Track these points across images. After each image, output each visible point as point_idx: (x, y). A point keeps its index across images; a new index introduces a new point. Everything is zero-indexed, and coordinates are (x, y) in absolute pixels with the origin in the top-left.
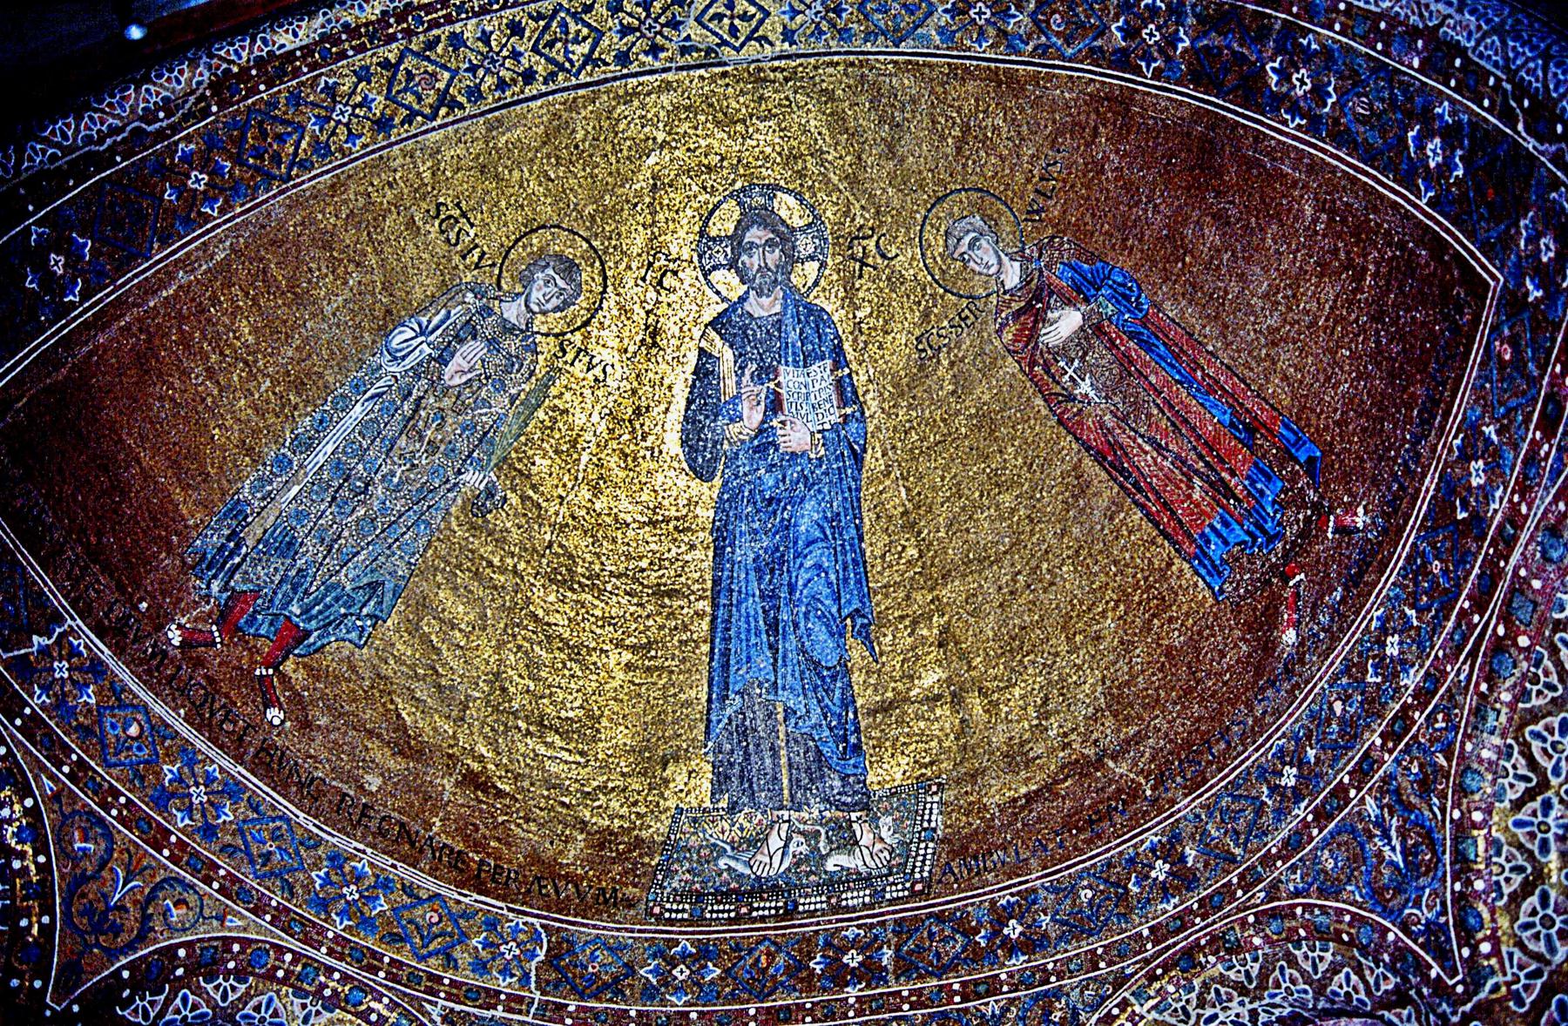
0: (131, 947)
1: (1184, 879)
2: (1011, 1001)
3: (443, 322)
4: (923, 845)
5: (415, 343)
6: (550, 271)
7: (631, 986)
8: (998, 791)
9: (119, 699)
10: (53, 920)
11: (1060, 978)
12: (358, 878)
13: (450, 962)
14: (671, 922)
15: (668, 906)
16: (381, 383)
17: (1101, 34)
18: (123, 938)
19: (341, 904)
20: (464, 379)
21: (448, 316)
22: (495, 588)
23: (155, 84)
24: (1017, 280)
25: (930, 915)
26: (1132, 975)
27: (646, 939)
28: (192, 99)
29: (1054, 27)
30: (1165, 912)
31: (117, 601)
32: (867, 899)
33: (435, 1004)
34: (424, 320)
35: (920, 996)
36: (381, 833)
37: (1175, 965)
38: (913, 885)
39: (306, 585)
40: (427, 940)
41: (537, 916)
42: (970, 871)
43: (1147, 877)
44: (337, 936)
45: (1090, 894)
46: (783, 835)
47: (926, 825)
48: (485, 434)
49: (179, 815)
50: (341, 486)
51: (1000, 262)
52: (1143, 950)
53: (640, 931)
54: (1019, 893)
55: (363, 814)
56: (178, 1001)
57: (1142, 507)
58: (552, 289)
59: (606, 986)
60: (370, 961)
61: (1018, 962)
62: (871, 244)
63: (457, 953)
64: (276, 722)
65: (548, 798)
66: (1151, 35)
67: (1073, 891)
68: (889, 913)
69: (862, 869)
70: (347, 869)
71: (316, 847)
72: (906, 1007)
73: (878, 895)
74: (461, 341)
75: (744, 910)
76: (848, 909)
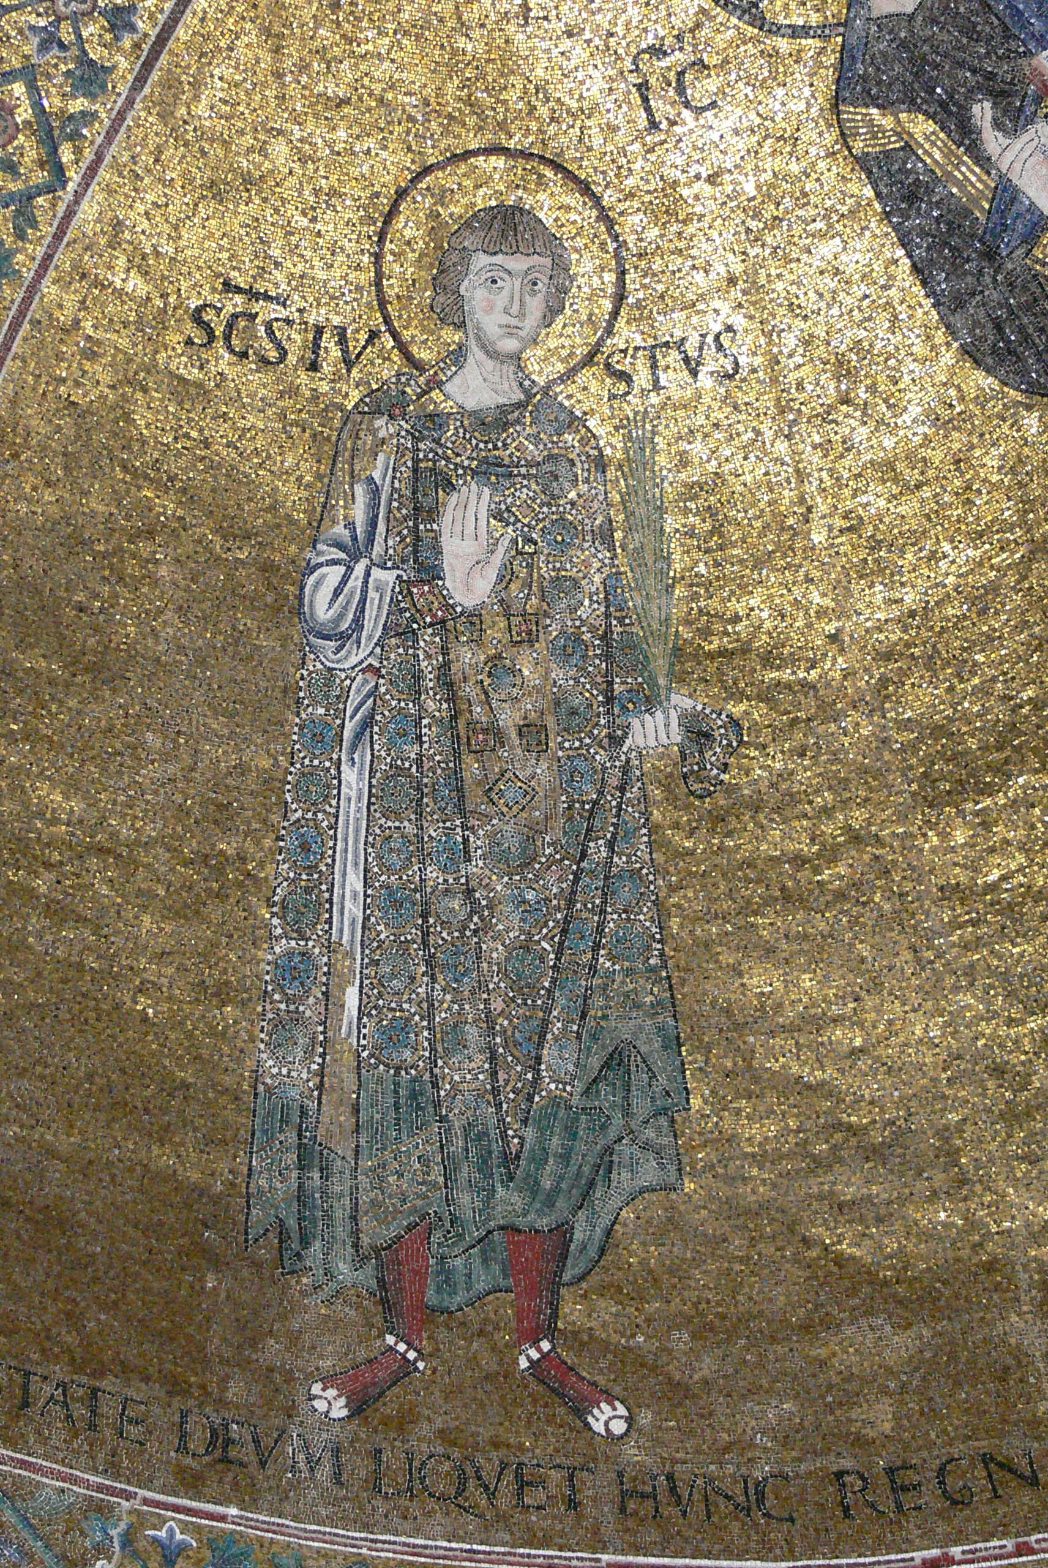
6: (481, 260)
20: (492, 574)
21: (375, 492)
31: (184, 1414)
34: (340, 531)
39: (496, 1148)
64: (619, 1427)
74: (433, 514)
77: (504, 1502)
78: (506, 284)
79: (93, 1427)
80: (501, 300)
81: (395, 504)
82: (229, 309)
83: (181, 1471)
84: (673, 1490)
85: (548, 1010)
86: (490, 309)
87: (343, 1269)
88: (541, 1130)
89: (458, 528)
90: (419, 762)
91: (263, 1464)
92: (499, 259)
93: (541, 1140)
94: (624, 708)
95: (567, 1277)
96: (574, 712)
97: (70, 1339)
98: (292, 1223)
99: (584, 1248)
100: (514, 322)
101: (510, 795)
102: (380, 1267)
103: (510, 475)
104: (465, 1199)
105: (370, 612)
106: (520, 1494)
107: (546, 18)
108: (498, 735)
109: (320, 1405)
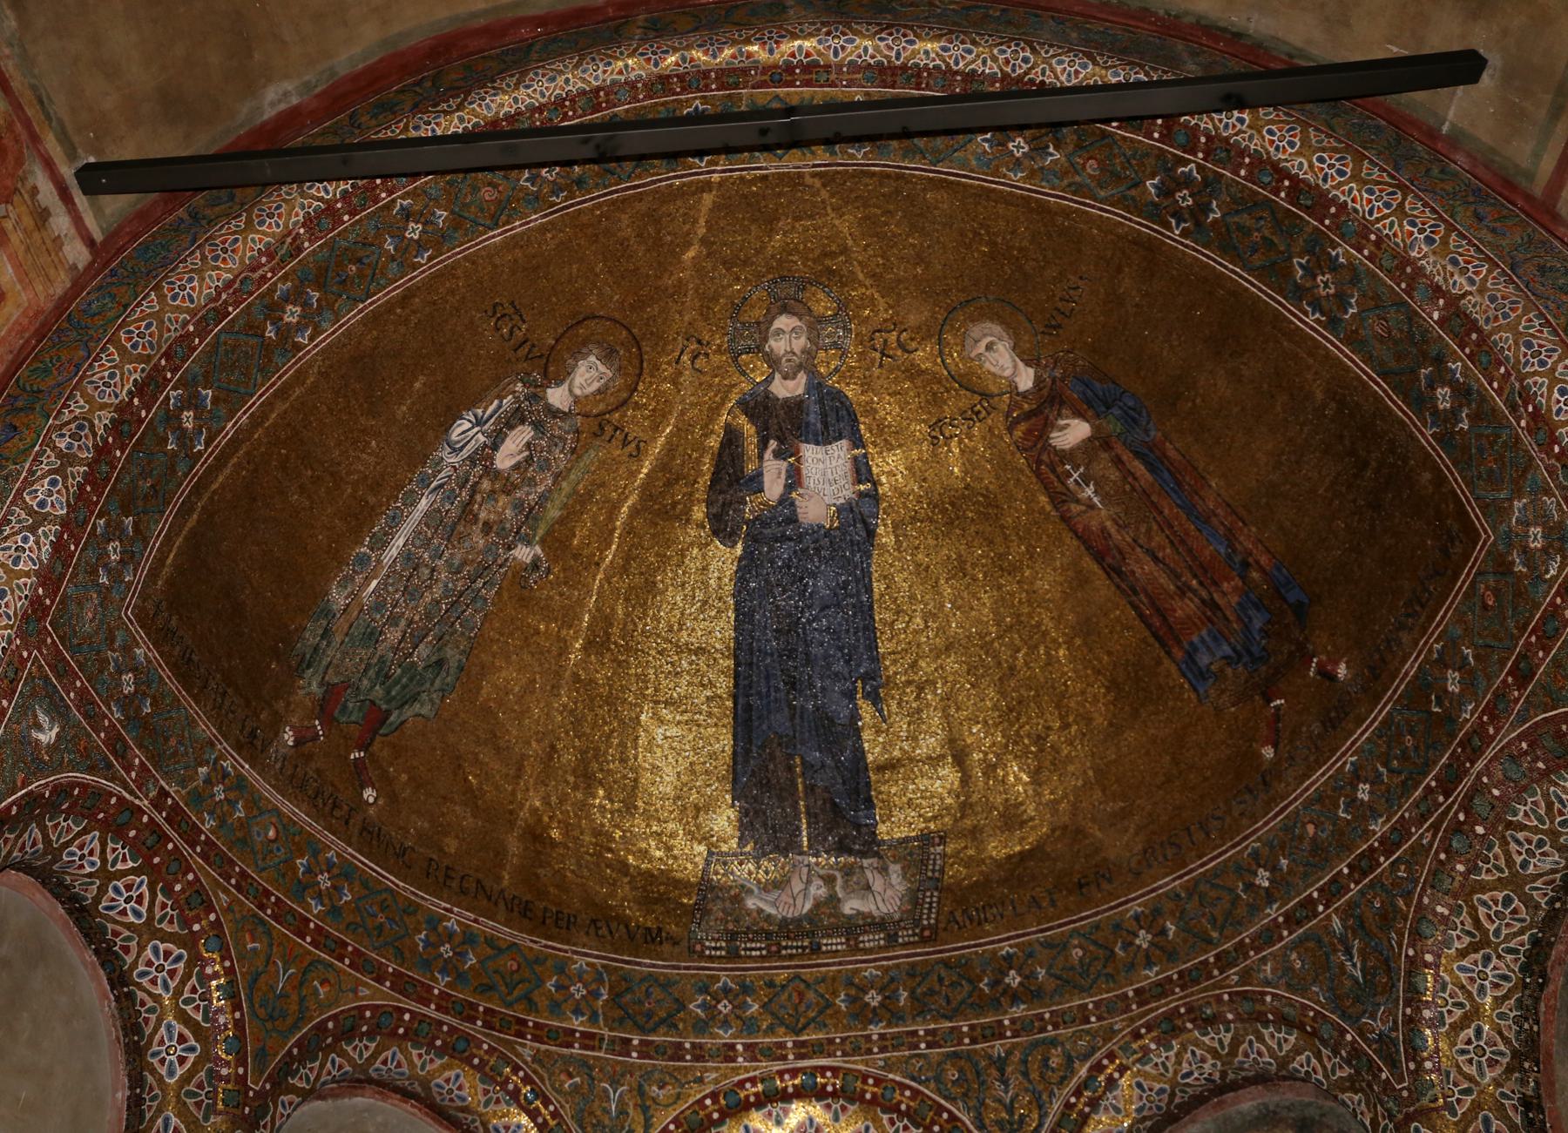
0: (295, 1027)
1: (1165, 952)
2: (1014, 1046)
3: (495, 412)
4: (928, 894)
5: (471, 433)
6: (592, 358)
7: (684, 1021)
8: (997, 848)
9: (259, 808)
10: (242, 1015)
11: (1056, 1027)
12: (450, 936)
13: (532, 1006)
14: (711, 958)
15: (707, 944)
16: (442, 474)
17: (1136, 185)
18: (289, 1021)
19: (441, 964)
20: (513, 462)
21: (500, 407)
22: (542, 653)
23: (258, 232)
25: (938, 961)
26: (1121, 1031)
27: (692, 976)
28: (289, 240)
29: (1089, 170)
30: (1148, 977)
31: (247, 717)
32: (882, 942)
33: (524, 1045)
34: (480, 412)
36: (464, 892)
37: (1159, 1026)
38: (923, 930)
40: (511, 987)
41: (597, 957)
42: (971, 921)
43: (1131, 944)
44: (441, 992)
45: (1080, 953)
46: (804, 878)
47: (930, 874)
48: (531, 509)
49: (313, 903)
50: (411, 576)
51: (1015, 367)
52: (1128, 1009)
54: (1016, 945)
55: (447, 876)
56: (329, 1065)
57: (1135, 607)
58: (593, 372)
59: (663, 1021)
60: (467, 1012)
61: (1019, 1011)
62: (893, 336)
63: (536, 996)
64: (371, 800)
65: (596, 844)
66: (1184, 198)
69: (876, 913)
70: (440, 929)
71: (415, 913)
72: (923, 1046)
73: (892, 939)
74: (512, 428)
75: (774, 948)
77: (327, 809)
79: (220, 708)
80: (587, 376)
82: (506, 311)
83: (238, 741)
84: (379, 835)
85: (430, 630)
86: (582, 376)
87: (314, 686)
88: (403, 672)
90: (447, 511)
91: (262, 751)
92: (598, 362)
93: (401, 677)
95: (381, 732)
96: (504, 529)
97: (226, 665)
98: (308, 656)
99: (391, 724)
101: (466, 544)
102: (326, 691)
104: (365, 682)
105: (468, 447)
106: (333, 809)
108: (476, 517)
109: (286, 737)
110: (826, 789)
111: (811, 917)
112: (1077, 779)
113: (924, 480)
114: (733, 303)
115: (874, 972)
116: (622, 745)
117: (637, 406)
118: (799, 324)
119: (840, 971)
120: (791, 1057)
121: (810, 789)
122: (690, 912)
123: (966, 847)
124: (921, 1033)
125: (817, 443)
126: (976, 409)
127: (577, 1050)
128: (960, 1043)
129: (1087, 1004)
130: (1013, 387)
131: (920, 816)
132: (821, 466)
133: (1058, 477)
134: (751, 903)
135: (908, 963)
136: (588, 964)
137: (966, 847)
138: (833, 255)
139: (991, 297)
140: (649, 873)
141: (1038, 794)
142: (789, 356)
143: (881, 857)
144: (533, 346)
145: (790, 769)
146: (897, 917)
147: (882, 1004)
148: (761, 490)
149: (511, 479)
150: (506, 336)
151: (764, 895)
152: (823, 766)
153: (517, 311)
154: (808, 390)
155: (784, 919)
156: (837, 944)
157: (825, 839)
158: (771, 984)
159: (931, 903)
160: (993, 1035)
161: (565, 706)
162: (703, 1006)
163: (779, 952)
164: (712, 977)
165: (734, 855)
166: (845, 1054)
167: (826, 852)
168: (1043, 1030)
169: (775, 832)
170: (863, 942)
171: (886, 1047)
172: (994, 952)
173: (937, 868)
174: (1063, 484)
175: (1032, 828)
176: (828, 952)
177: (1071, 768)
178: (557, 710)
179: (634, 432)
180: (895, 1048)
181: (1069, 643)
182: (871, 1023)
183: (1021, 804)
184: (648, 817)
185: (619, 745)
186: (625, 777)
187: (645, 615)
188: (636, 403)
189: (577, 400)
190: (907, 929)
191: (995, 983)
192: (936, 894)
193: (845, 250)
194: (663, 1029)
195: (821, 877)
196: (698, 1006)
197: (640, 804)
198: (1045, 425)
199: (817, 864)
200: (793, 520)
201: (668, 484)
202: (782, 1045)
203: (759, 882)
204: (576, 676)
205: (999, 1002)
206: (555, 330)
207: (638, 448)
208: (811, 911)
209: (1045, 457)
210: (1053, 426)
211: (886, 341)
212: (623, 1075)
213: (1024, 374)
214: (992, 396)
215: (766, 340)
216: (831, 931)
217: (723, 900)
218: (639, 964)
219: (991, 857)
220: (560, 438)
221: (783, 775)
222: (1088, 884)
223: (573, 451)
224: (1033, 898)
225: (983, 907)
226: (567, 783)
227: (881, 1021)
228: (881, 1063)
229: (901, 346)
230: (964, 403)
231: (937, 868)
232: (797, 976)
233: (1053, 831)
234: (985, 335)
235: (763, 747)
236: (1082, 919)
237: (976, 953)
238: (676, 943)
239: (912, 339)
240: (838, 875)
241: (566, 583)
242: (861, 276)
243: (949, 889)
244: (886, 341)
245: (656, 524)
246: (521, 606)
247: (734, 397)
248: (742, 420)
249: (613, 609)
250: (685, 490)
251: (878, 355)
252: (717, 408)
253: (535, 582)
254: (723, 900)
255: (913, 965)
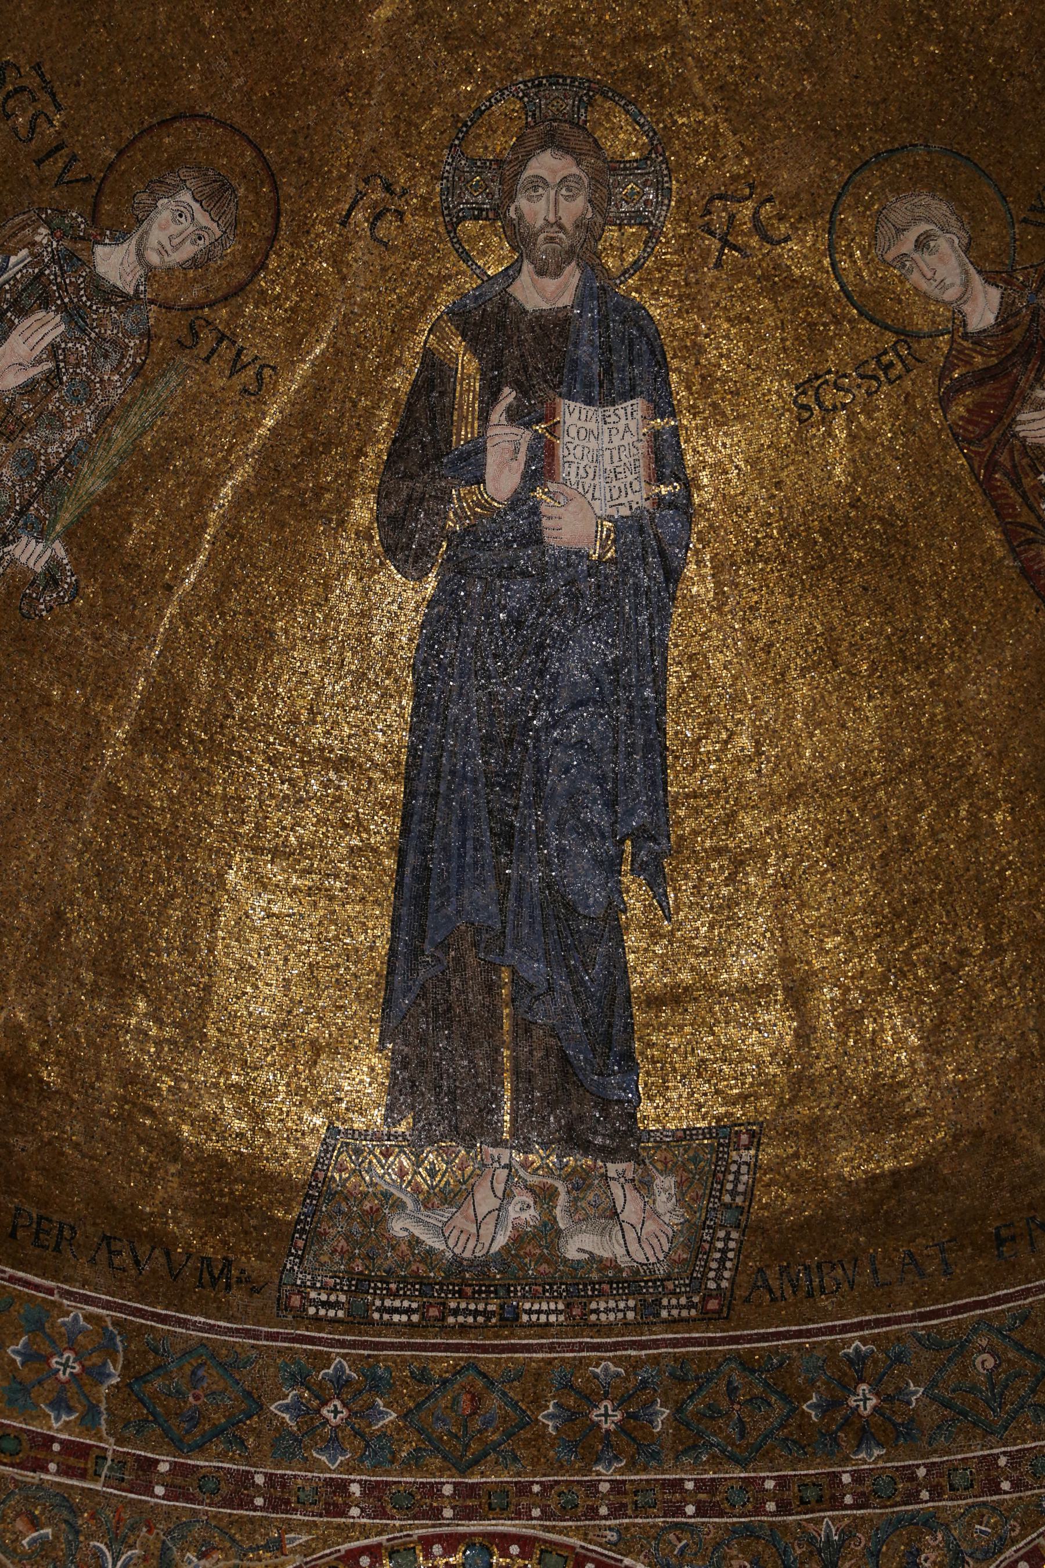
2: (858, 1523)
4: (722, 1234)
6: (186, 197)
11: (936, 1493)
15: (313, 1295)
20: (22, 378)
24: (990, 318)
25: (728, 1357)
27: (280, 1351)
32: (630, 1315)
35: (712, 1492)
38: (704, 1300)
41: (107, 1305)
42: (795, 1288)
45: (990, 1363)
46: (500, 1188)
47: (727, 1198)
48: (51, 472)
51: (966, 284)
53: (270, 1337)
54: (874, 1339)
59: (218, 1432)
62: (746, 210)
65: (124, 1100)
67: (962, 1349)
68: (666, 1343)
69: (623, 1261)
72: (690, 1509)
73: (649, 1310)
74: (24, 312)
75: (434, 1312)
76: (599, 1329)
78: (185, 223)
80: (174, 229)
81: (7, 287)
82: (26, 82)
86: (162, 228)
89: (27, 334)
92: (196, 206)
94: (25, 524)
100: (168, 248)
103: (83, 331)
107: (351, 104)
110: (553, 1032)
111: (505, 1258)
112: (1009, 1047)
113: (778, 485)
114: (456, 119)
115: (612, 1368)
116: (188, 922)
117: (262, 296)
118: (575, 170)
119: (550, 1362)
120: (448, 1513)
121: (524, 1028)
122: (286, 1234)
123: (796, 1155)
124: (690, 1486)
125: (589, 401)
126: (885, 359)
127: (51, 1476)
128: (759, 1510)
129: (996, 1457)
130: (958, 318)
131: (717, 1092)
132: (593, 444)
133: (1024, 496)
134: (399, 1227)
135: (676, 1358)
136: (88, 1318)
137: (796, 1155)
138: (649, 41)
139: (936, 146)
140: (217, 1155)
141: (936, 1070)
142: (552, 232)
143: (640, 1162)
144: (74, 158)
145: (491, 988)
146: (661, 1271)
147: (621, 1427)
148: (480, 480)
149: (18, 411)
150: (23, 132)
151: (423, 1214)
152: (550, 989)
153: (46, 86)
154: (580, 301)
155: (458, 1260)
156: (548, 1312)
157: (544, 1121)
158: (422, 1377)
159: (724, 1251)
160: (819, 1500)
161: (87, 843)
162: (296, 1408)
163: (443, 1319)
164: (316, 1355)
165: (377, 1137)
166: (546, 1515)
167: (544, 1145)
168: (912, 1497)
169: (453, 1101)
170: (597, 1311)
171: (624, 1506)
172: (833, 1349)
173: (741, 1188)
174: (1032, 508)
175: (921, 1130)
176: (531, 1325)
177: (998, 1027)
178: (73, 848)
179: (255, 347)
180: (639, 1510)
181: (1015, 802)
182: (598, 1461)
183: (902, 1085)
184: (223, 1055)
185: (181, 921)
186: (187, 980)
187: (250, 689)
188: (263, 292)
189: (150, 274)
190: (678, 1295)
191: (831, 1405)
192: (734, 1235)
193: (672, 34)
194: (218, 1446)
195: (530, 1189)
196: (287, 1408)
197: (212, 1032)
198: (1010, 397)
199: (525, 1165)
200: (534, 537)
201: (310, 451)
202: (433, 1491)
203: (417, 1190)
204: (112, 791)
205: (835, 1440)
206: (118, 131)
207: (259, 377)
208: (506, 1248)
209: (1003, 458)
210: (1024, 399)
211: (732, 217)
212: (133, 1528)
213: (981, 299)
214: (918, 337)
215: (511, 197)
216: (543, 1289)
217: (349, 1217)
218: (183, 1323)
219: (840, 1177)
220: (114, 342)
221: (476, 998)
222: (1013, 1238)
223: (138, 371)
224: (911, 1255)
225: (819, 1266)
226: (78, 980)
227: (617, 1458)
228: (612, 1536)
229: (759, 228)
230: (865, 349)
231: (741, 1188)
232: (472, 1365)
233: (956, 1138)
234: (916, 220)
235: (444, 946)
236: (997, 1301)
237: (800, 1347)
238: (254, 1291)
239: (781, 218)
240: (561, 1187)
241: (107, 617)
242: (698, 87)
243: (760, 1229)
244: (732, 217)
245: (283, 525)
246: (20, 651)
247: (444, 301)
248: (457, 344)
249: (190, 674)
250: (341, 465)
251: (716, 244)
252: (412, 317)
253: (49, 610)
254: (349, 1217)
255: (682, 1360)
